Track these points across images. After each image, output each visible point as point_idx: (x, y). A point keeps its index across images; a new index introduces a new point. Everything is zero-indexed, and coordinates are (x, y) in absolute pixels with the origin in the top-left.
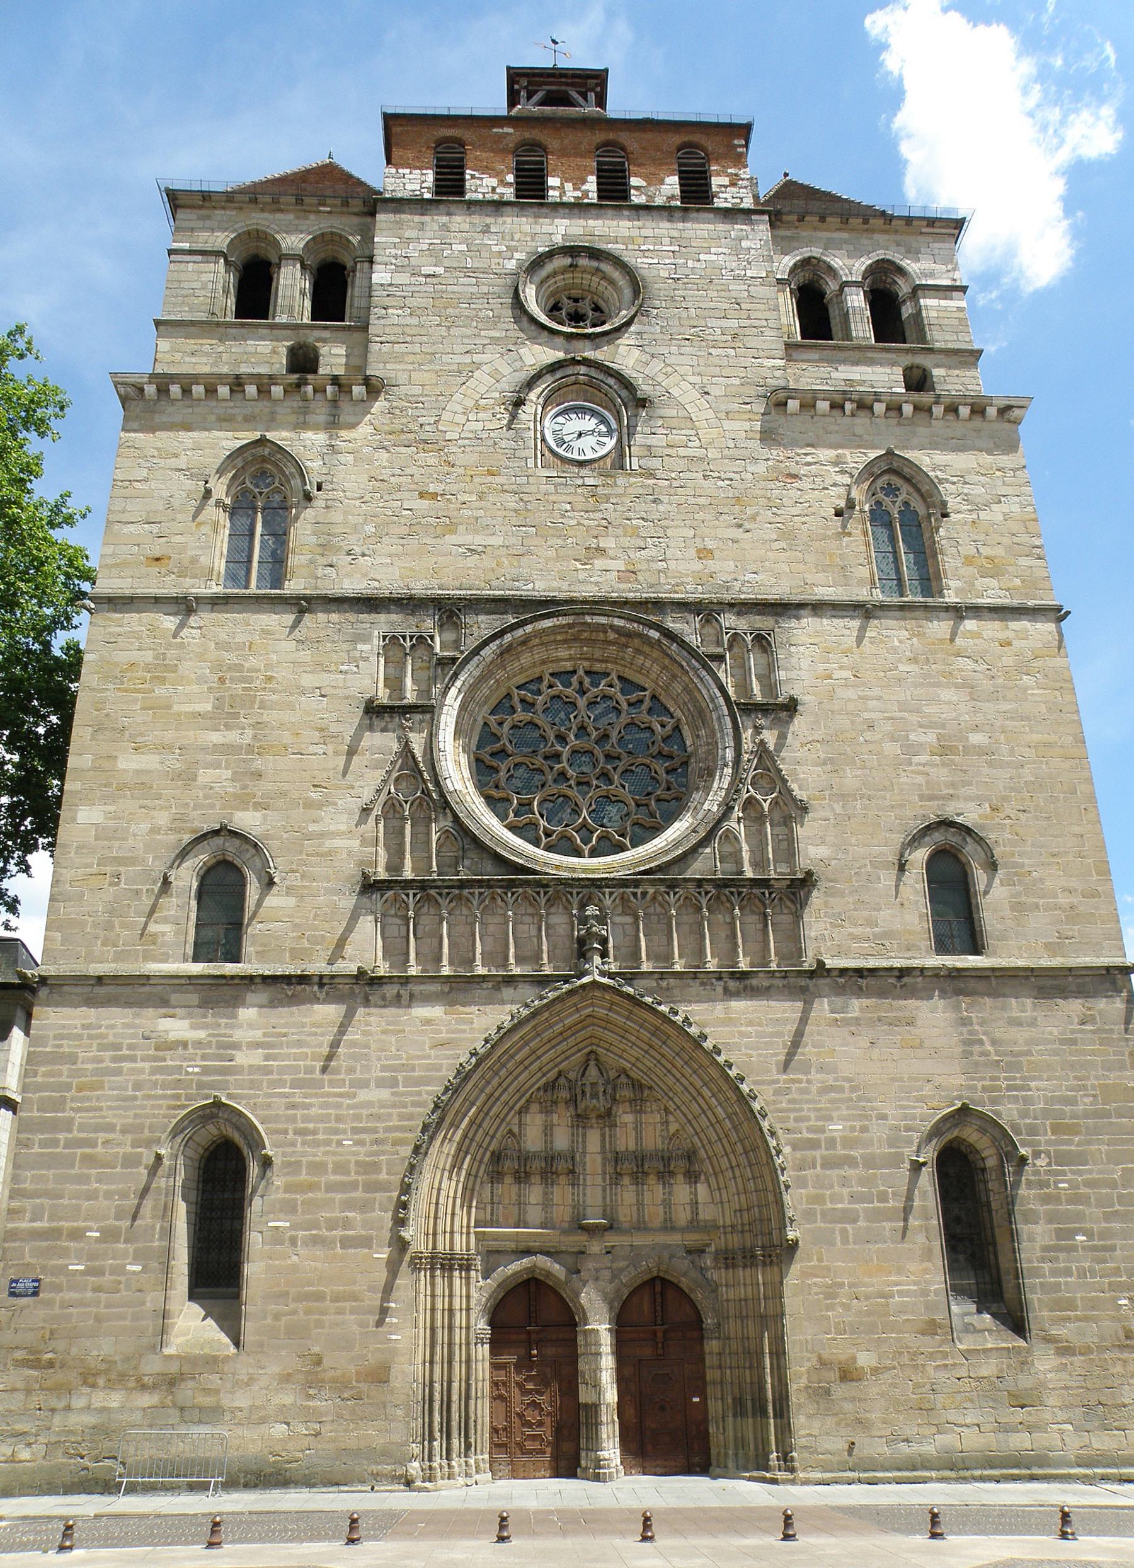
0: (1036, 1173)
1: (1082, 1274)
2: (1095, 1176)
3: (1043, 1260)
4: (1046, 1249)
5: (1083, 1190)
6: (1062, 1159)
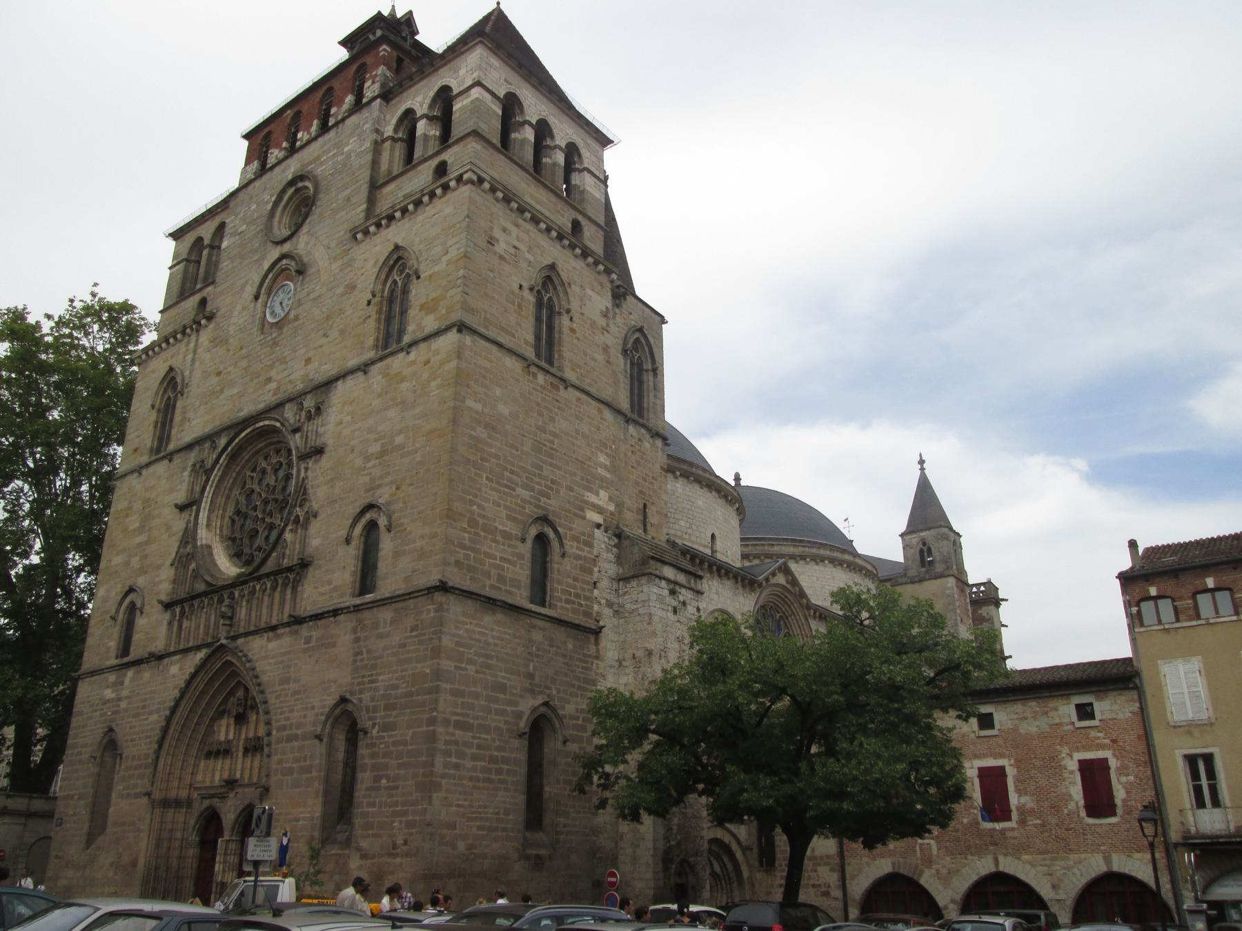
0: (372, 738)
1: (380, 807)
2: (399, 738)
3: (365, 797)
4: (367, 789)
5: (392, 748)
6: (386, 727)
